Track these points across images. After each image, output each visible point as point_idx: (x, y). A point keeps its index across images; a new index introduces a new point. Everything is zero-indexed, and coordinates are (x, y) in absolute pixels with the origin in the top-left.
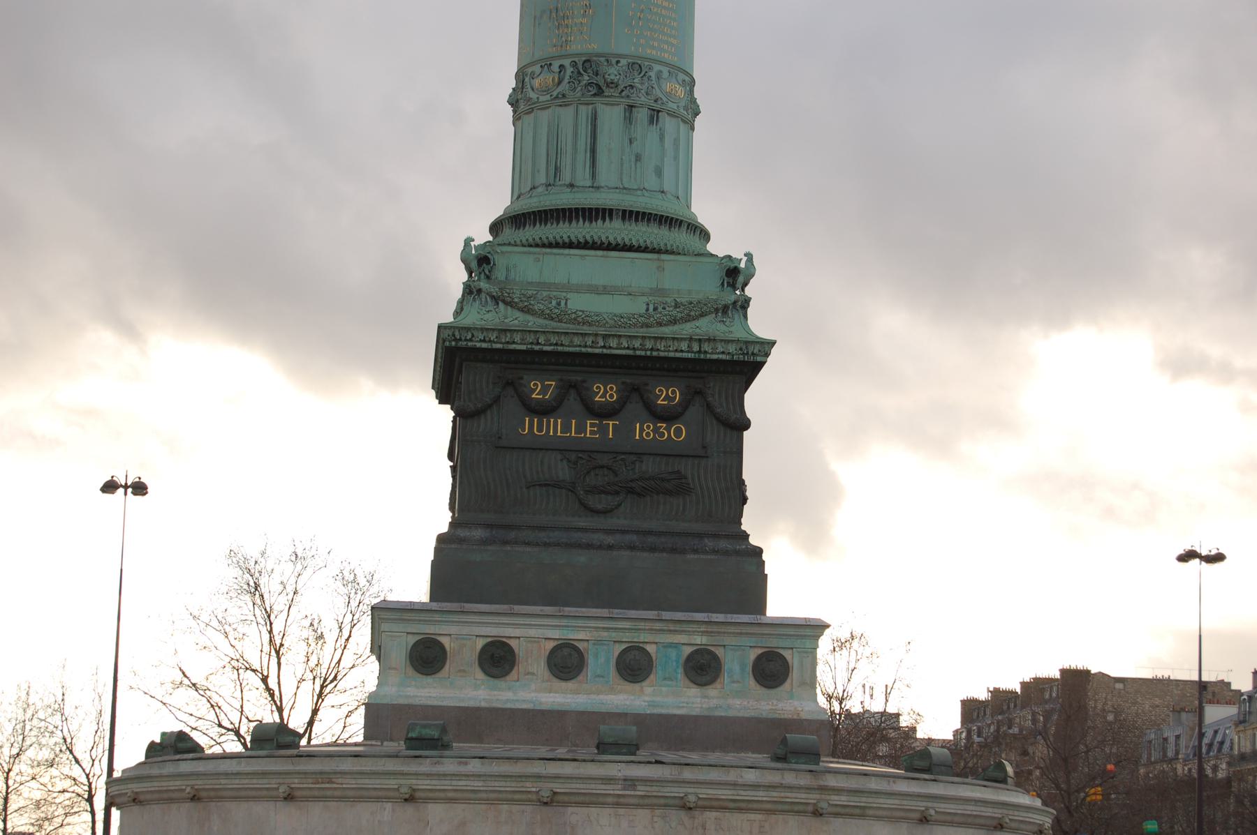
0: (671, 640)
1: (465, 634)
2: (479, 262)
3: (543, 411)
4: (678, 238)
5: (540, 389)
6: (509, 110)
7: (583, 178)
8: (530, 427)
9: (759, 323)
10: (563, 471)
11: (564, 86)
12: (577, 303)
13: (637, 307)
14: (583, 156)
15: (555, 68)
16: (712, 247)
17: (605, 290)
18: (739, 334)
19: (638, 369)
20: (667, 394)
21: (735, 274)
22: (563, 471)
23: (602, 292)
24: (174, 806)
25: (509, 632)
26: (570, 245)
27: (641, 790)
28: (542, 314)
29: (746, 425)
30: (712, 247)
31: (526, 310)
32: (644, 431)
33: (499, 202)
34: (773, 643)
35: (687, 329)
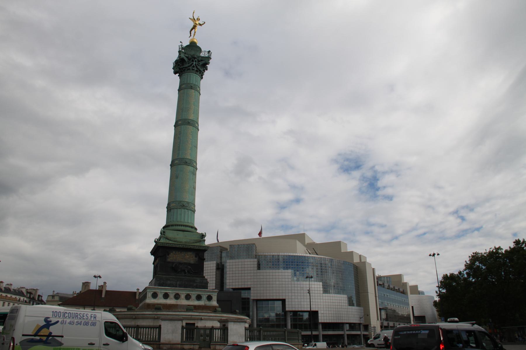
0: (194, 293)
1: (161, 292)
2: (163, 233)
4: (193, 230)
6: (166, 209)
16: (198, 231)
18: (203, 245)
21: (203, 236)
23: (181, 238)
30: (198, 231)
31: (171, 240)
33: (164, 223)
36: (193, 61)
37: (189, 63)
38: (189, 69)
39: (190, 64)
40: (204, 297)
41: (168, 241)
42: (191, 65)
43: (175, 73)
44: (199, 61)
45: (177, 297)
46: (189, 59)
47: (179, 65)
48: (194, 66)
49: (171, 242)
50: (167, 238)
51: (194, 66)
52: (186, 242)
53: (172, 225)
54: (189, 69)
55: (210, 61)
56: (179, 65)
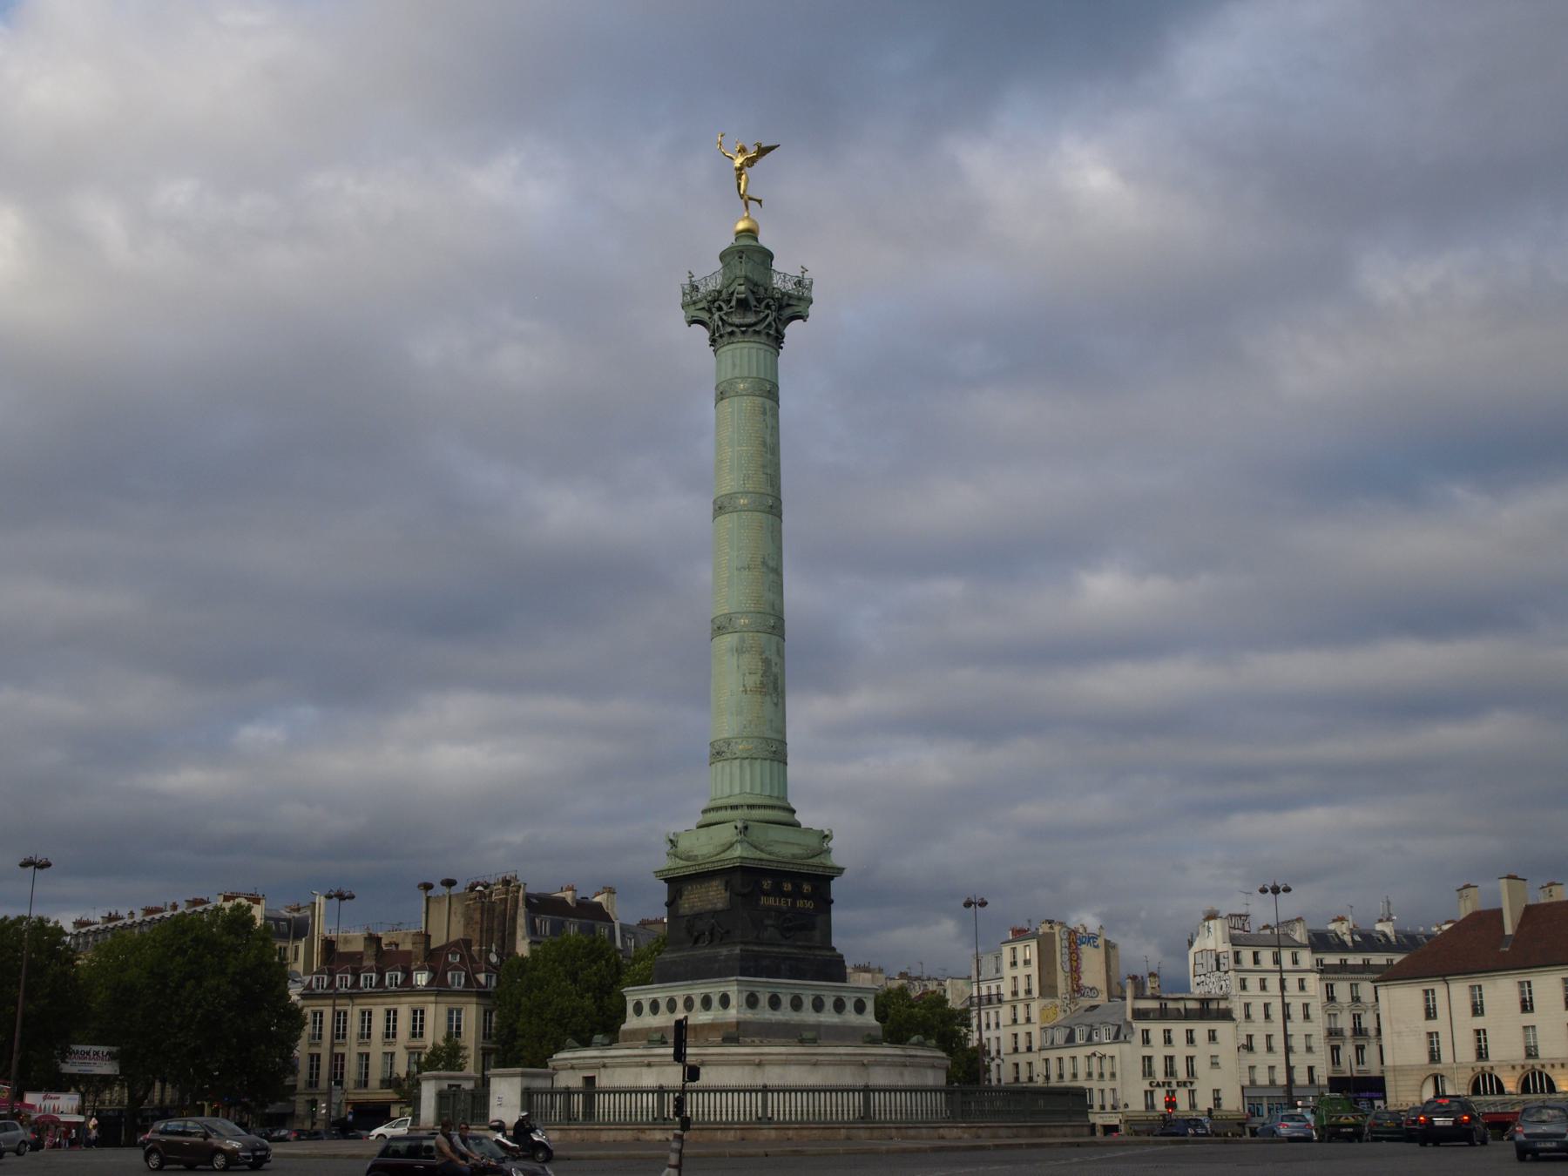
3: (767, 894)
5: (767, 884)
8: (763, 900)
9: (836, 859)
12: (776, 849)
13: (796, 850)
19: (797, 877)
20: (807, 888)
32: (800, 903)
35: (811, 861)
36: (768, 306)
38: (758, 333)
40: (850, 1005)
41: (758, 855)
43: (694, 321)
44: (781, 308)
45: (797, 1004)
46: (759, 301)
47: (720, 309)
49: (764, 856)
51: (769, 325)
52: (794, 856)
53: (751, 807)
54: (758, 333)
55: (812, 310)
56: (720, 309)
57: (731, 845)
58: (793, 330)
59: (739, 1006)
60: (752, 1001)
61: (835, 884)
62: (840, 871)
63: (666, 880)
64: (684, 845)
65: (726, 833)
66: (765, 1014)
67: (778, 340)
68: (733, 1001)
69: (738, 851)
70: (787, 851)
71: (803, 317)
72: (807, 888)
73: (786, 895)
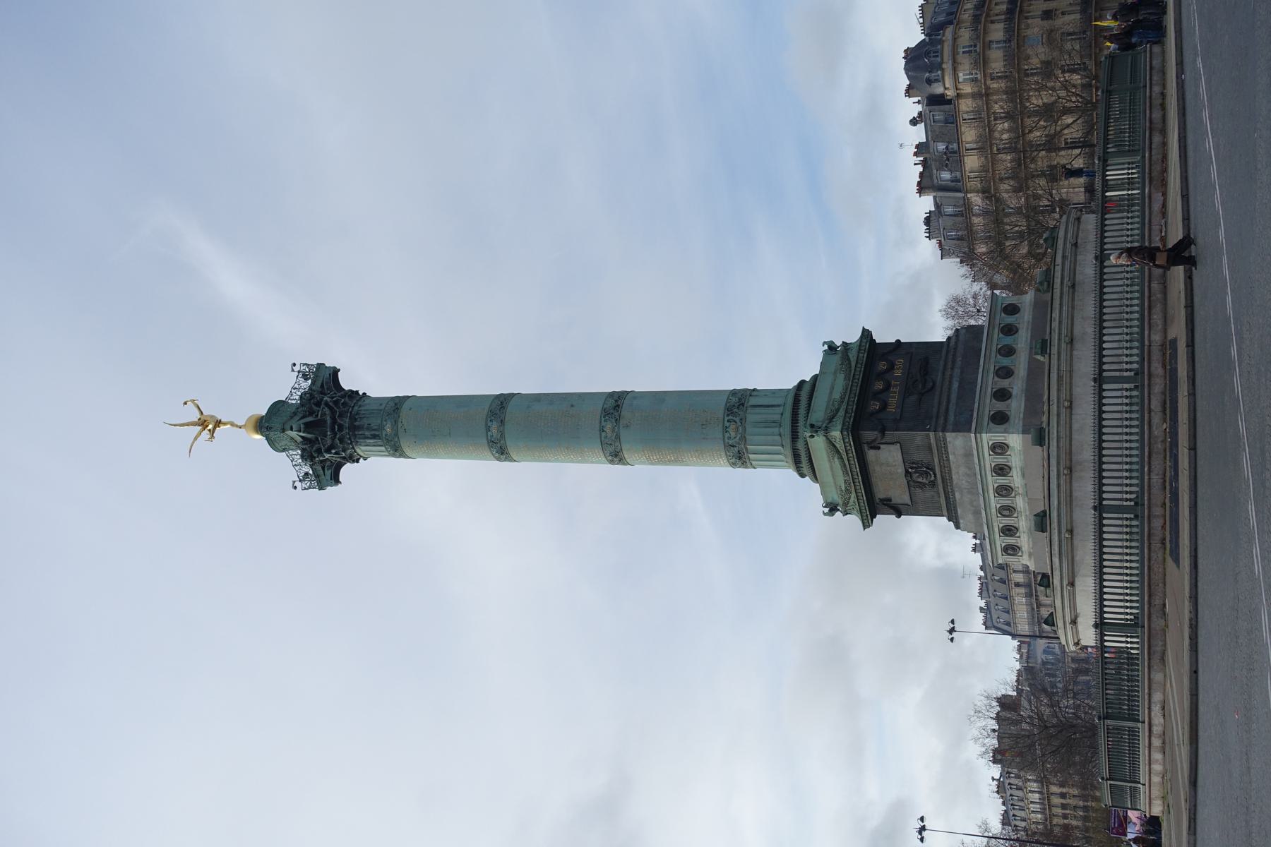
3: (884, 406)
7: (779, 410)
8: (891, 409)
9: (853, 337)
10: (913, 398)
11: (737, 419)
12: (837, 395)
13: (841, 377)
14: (770, 410)
15: (727, 424)
17: (832, 388)
20: (882, 366)
22: (913, 398)
24: (1075, 494)
25: (987, 412)
26: (809, 405)
27: (1068, 253)
28: (840, 405)
29: (898, 341)
31: (837, 410)
34: (999, 309)
37: (324, 414)
39: (327, 411)
41: (842, 413)
42: (331, 408)
46: (311, 413)
48: (336, 403)
50: (831, 419)
57: (832, 444)
58: (346, 383)
59: (1006, 431)
60: (1000, 419)
61: (883, 336)
62: (866, 334)
63: (873, 516)
64: (837, 498)
65: (818, 444)
66: (1016, 406)
67: (353, 394)
68: (999, 438)
69: (836, 434)
70: (841, 382)
71: (335, 372)
72: (882, 366)
73: (888, 387)
